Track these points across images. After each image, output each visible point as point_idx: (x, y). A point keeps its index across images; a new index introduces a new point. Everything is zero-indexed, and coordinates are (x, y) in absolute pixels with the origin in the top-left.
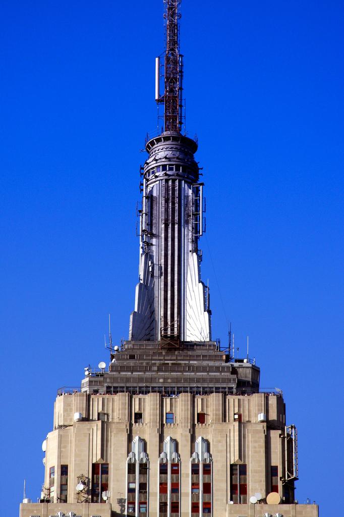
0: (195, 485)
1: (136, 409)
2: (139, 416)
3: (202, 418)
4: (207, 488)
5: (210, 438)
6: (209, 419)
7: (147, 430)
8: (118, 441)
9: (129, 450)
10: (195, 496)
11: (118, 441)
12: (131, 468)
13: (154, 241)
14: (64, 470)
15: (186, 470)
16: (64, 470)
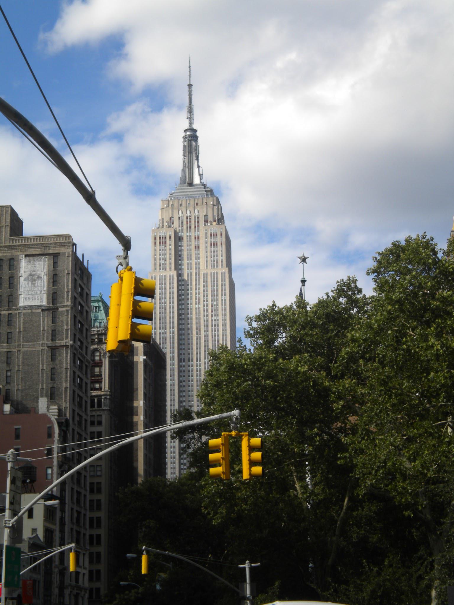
0: (195, 221)
1: (180, 203)
2: (181, 205)
3: (197, 204)
4: (198, 222)
5: (199, 209)
6: (199, 204)
7: (183, 208)
8: (176, 212)
9: (179, 214)
10: (195, 224)
11: (176, 212)
12: (179, 218)
13: (186, 158)
14: (163, 219)
15: (193, 218)
16: (163, 219)
